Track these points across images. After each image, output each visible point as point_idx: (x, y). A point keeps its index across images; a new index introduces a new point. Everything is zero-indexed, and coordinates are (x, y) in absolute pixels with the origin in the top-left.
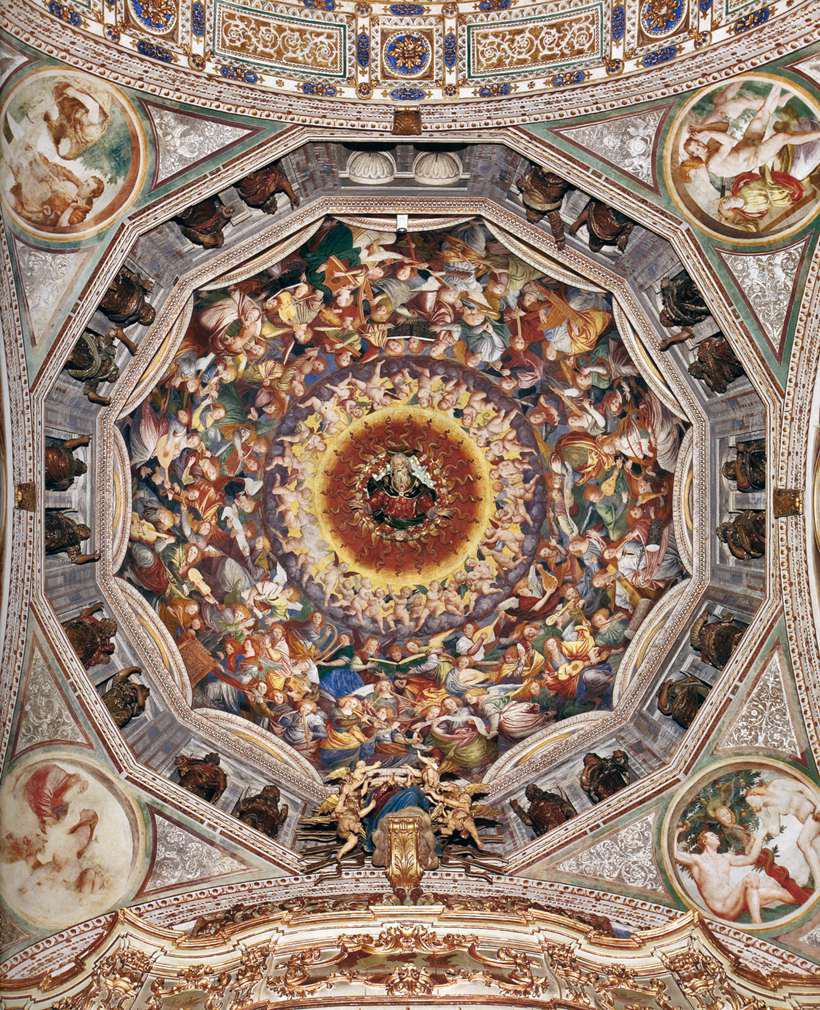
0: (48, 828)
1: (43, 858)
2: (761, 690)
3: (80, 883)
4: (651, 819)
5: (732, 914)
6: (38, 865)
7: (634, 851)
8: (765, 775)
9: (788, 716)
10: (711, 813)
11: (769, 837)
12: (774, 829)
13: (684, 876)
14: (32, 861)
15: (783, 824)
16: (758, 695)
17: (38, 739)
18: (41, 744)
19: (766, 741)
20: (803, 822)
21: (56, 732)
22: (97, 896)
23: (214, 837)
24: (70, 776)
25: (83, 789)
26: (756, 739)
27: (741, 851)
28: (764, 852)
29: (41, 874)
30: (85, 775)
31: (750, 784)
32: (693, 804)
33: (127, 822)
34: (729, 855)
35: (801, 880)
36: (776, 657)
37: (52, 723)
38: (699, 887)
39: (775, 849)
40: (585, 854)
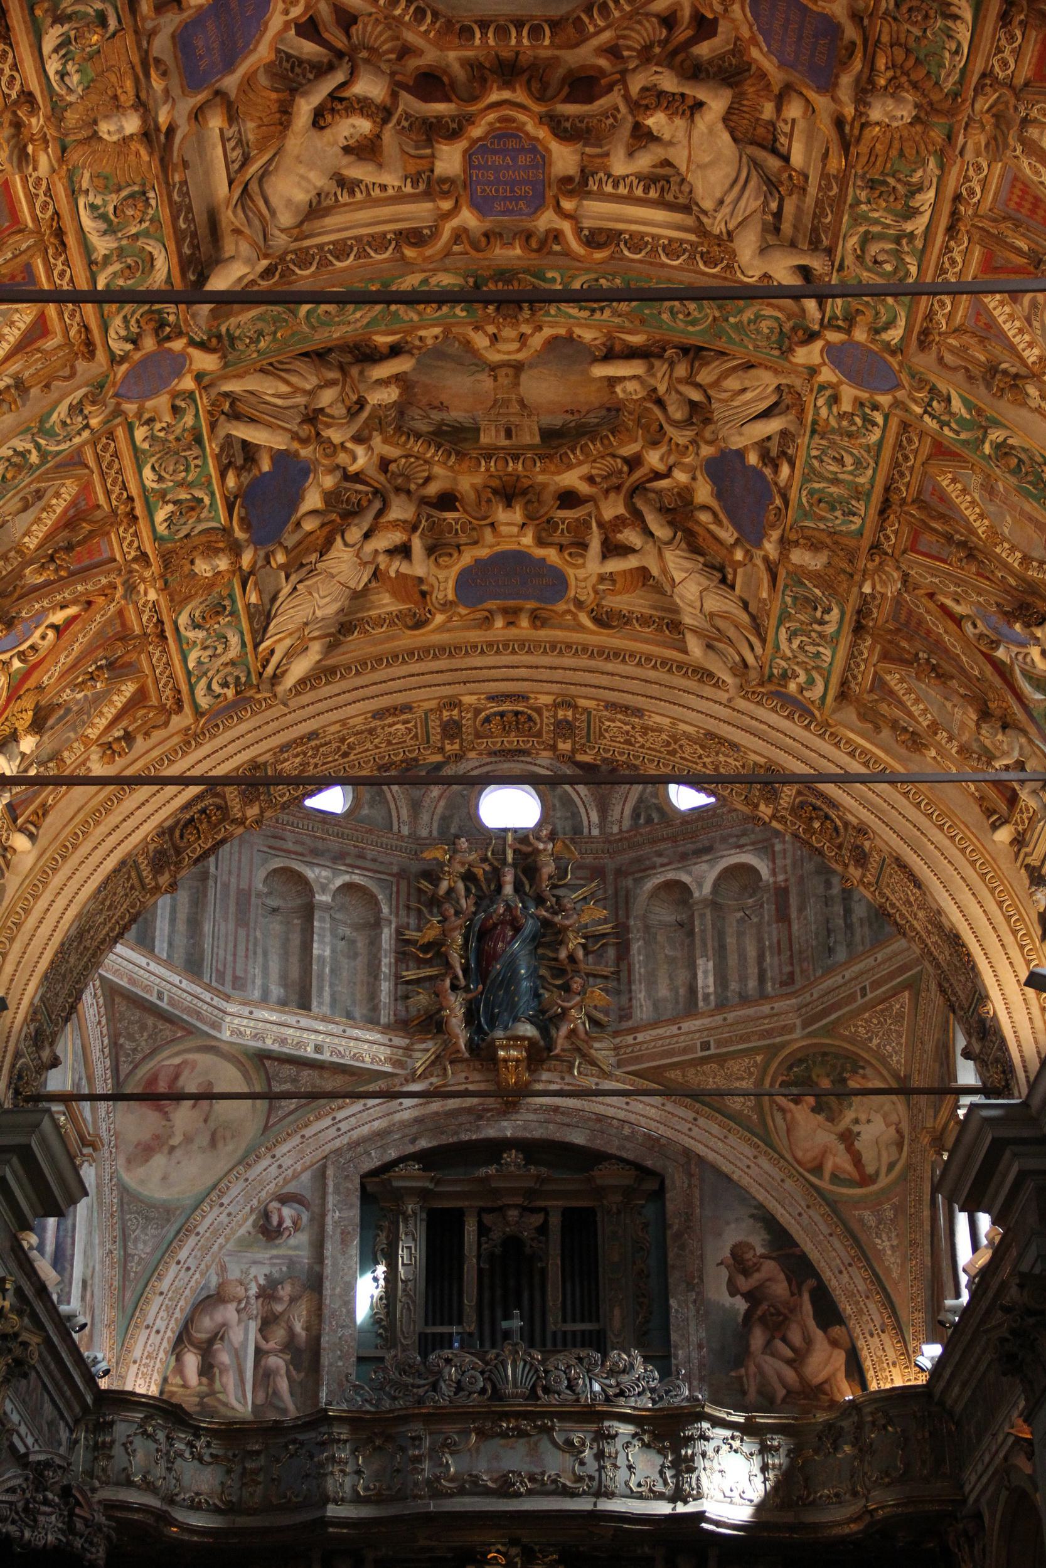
0: (171, 1116)
1: (174, 1141)
2: (887, 1009)
3: (213, 1143)
4: (759, 1059)
5: (809, 1166)
6: (173, 1149)
7: (738, 1079)
8: (869, 1071)
9: (903, 1040)
10: (814, 1077)
11: (857, 1121)
12: (863, 1117)
13: (778, 1116)
14: (166, 1149)
15: (872, 1117)
16: (882, 1011)
17: (139, 1056)
18: (144, 1059)
19: (878, 1045)
20: (888, 1125)
21: (155, 1040)
22: (230, 1147)
23: (324, 1062)
24: (179, 1065)
25: (193, 1068)
26: (870, 1039)
27: (831, 1119)
28: (849, 1131)
29: (178, 1153)
30: (190, 1056)
31: (854, 1072)
32: (801, 1061)
33: (239, 1075)
34: (820, 1118)
35: (870, 1170)
36: (906, 994)
37: (150, 1036)
38: (788, 1131)
39: (859, 1134)
40: (692, 1071)
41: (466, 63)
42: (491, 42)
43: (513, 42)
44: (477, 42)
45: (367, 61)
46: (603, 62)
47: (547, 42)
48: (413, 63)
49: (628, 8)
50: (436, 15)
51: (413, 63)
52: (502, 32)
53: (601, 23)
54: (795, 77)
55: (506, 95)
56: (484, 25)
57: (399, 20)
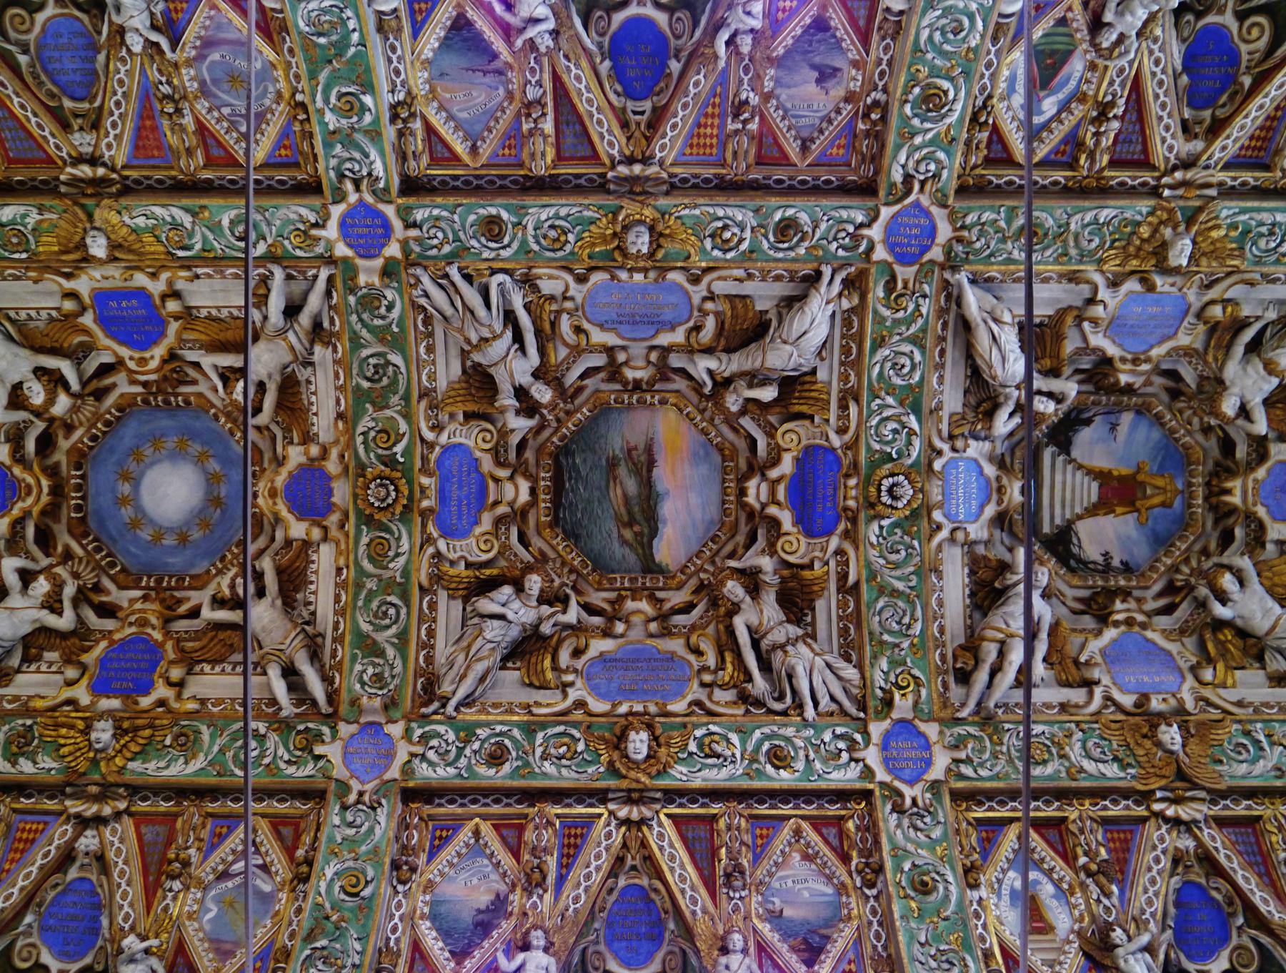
41: (57, 465)
42: (73, 481)
43: (73, 495)
44: (73, 473)
45: (74, 405)
46: (60, 549)
47: (73, 515)
48: (61, 434)
49: (103, 563)
50: (91, 448)
51: (61, 434)
52: (78, 488)
53: (90, 547)
54: (93, 670)
55: (46, 490)
56: (83, 477)
57: (94, 425)
